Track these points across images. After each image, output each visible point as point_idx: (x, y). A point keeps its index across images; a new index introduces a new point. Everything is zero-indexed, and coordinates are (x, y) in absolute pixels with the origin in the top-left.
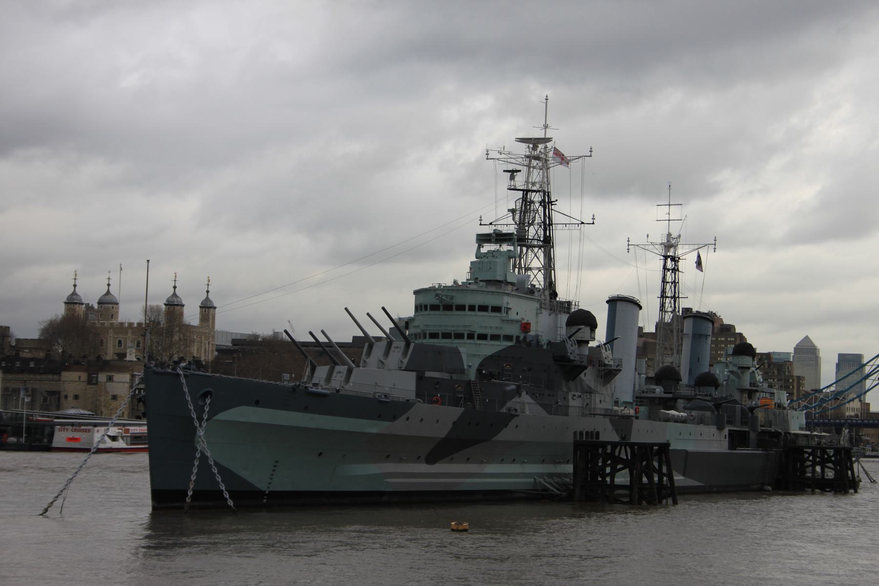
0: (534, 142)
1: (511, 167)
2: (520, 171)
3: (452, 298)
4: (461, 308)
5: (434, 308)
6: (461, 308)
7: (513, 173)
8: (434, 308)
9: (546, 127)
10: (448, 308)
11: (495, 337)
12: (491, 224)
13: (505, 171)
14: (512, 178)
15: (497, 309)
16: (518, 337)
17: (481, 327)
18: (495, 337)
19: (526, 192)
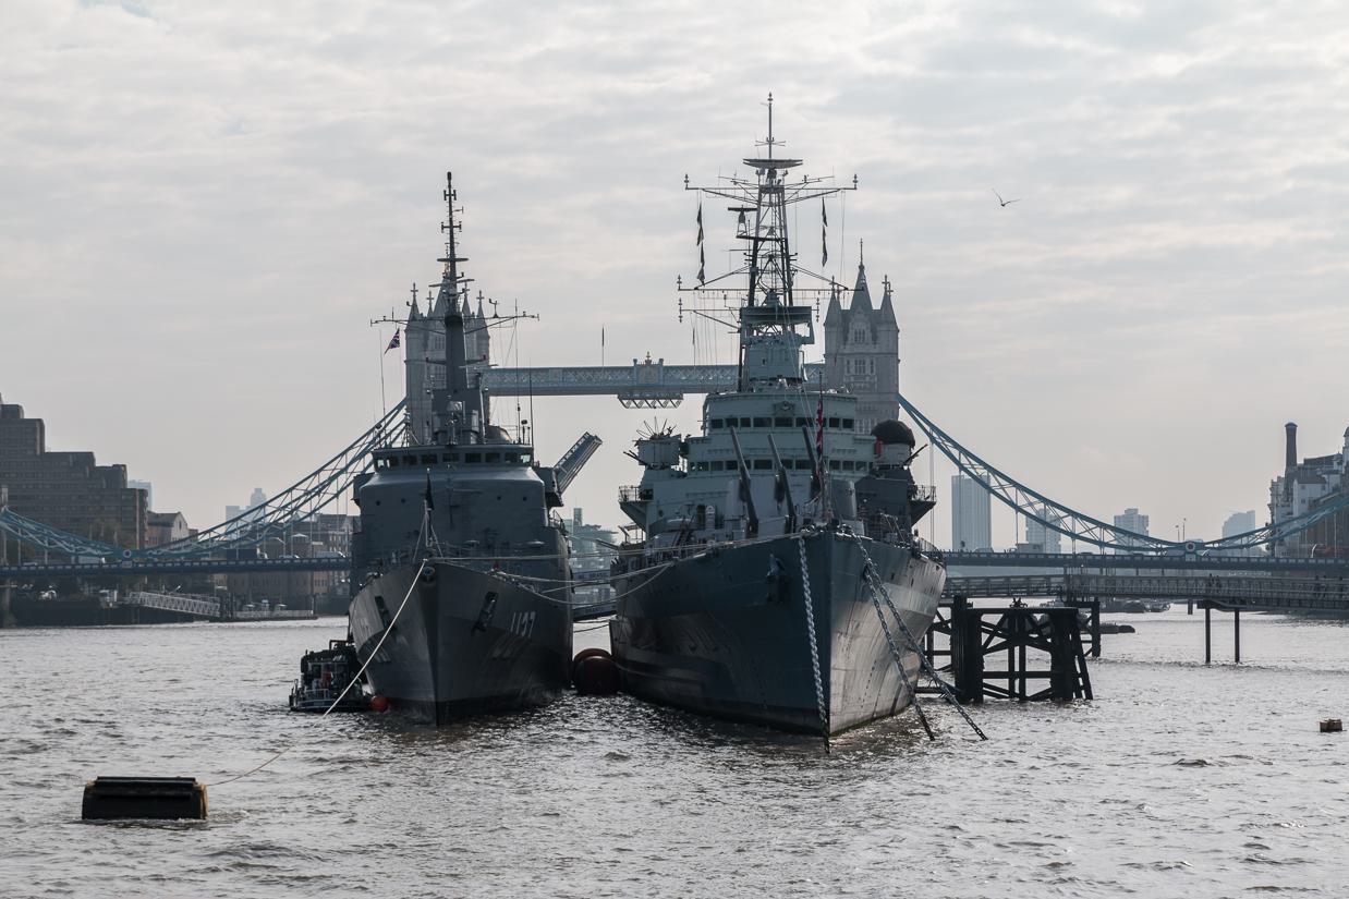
0: (769, 166)
1: (738, 204)
2: (753, 209)
3: (793, 406)
7: (742, 210)
8: (760, 422)
9: (770, 141)
10: (783, 422)
11: (848, 465)
12: (696, 289)
13: (729, 209)
14: (742, 219)
15: (849, 423)
16: (871, 464)
17: (833, 450)
18: (848, 465)
19: (757, 240)
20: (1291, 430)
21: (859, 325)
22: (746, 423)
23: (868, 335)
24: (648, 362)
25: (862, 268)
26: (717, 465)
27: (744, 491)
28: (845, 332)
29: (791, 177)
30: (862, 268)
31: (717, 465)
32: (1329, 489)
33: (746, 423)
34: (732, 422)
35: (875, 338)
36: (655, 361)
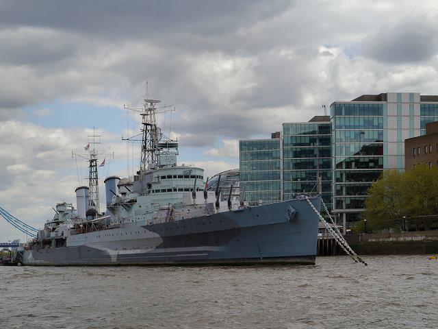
0: (152, 102)
5: (180, 177)
6: (193, 177)
7: (144, 115)
8: (180, 177)
10: (187, 177)
14: (144, 118)
19: (146, 124)
22: (175, 177)
26: (164, 191)
27: (194, 195)
29: (157, 106)
31: (164, 191)
33: (175, 177)
34: (170, 177)
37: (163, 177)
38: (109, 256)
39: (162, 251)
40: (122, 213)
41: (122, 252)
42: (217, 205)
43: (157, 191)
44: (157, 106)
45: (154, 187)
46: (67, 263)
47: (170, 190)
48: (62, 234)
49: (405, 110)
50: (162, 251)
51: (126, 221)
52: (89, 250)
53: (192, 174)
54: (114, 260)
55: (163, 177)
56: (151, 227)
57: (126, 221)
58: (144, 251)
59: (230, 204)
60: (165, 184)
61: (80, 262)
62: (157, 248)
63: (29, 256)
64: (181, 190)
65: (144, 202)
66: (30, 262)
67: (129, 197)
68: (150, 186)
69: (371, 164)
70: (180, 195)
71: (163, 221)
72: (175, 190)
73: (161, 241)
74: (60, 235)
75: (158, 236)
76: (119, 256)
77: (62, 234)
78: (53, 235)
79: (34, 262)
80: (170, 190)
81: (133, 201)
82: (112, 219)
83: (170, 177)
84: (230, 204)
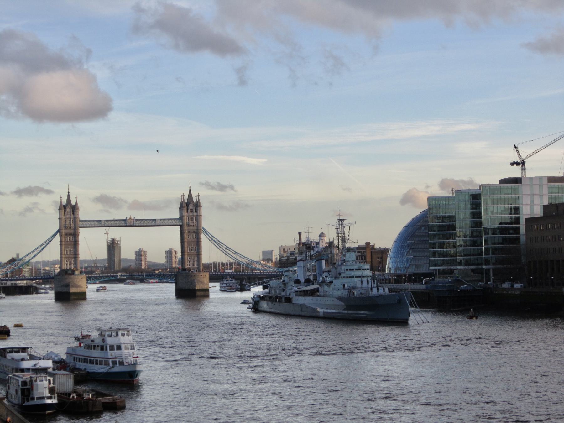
0: (342, 220)
4: (363, 269)
5: (356, 270)
6: (363, 269)
8: (356, 270)
10: (360, 269)
20: (300, 234)
21: (191, 207)
22: (353, 270)
23: (194, 210)
24: (130, 219)
25: (190, 191)
26: (348, 277)
27: (362, 282)
28: (188, 209)
30: (190, 191)
31: (348, 277)
32: (315, 252)
33: (353, 270)
34: (350, 270)
35: (196, 211)
36: (132, 218)
37: (347, 270)
38: (319, 312)
39: (346, 312)
40: (326, 288)
41: (326, 311)
42: (371, 289)
43: (344, 277)
44: (345, 222)
45: (343, 275)
46: (293, 313)
47: (350, 277)
48: (290, 295)
49: (536, 190)
50: (346, 312)
51: (327, 293)
52: (307, 307)
53: (363, 268)
54: (321, 315)
55: (347, 270)
56: (339, 299)
57: (327, 293)
58: (337, 311)
59: (378, 289)
60: (348, 273)
61: (303, 314)
62: (344, 310)
63: (264, 305)
64: (357, 277)
65: (338, 283)
66: (266, 310)
67: (328, 280)
68: (340, 274)
69: (511, 232)
70: (356, 280)
71: (346, 296)
72: (353, 277)
73: (345, 307)
74: (288, 294)
75: (343, 304)
76: (324, 312)
77: (290, 295)
78: (283, 294)
79: (268, 310)
80: (350, 277)
81: (331, 282)
82: (320, 289)
83: (350, 270)
84: (378, 289)
